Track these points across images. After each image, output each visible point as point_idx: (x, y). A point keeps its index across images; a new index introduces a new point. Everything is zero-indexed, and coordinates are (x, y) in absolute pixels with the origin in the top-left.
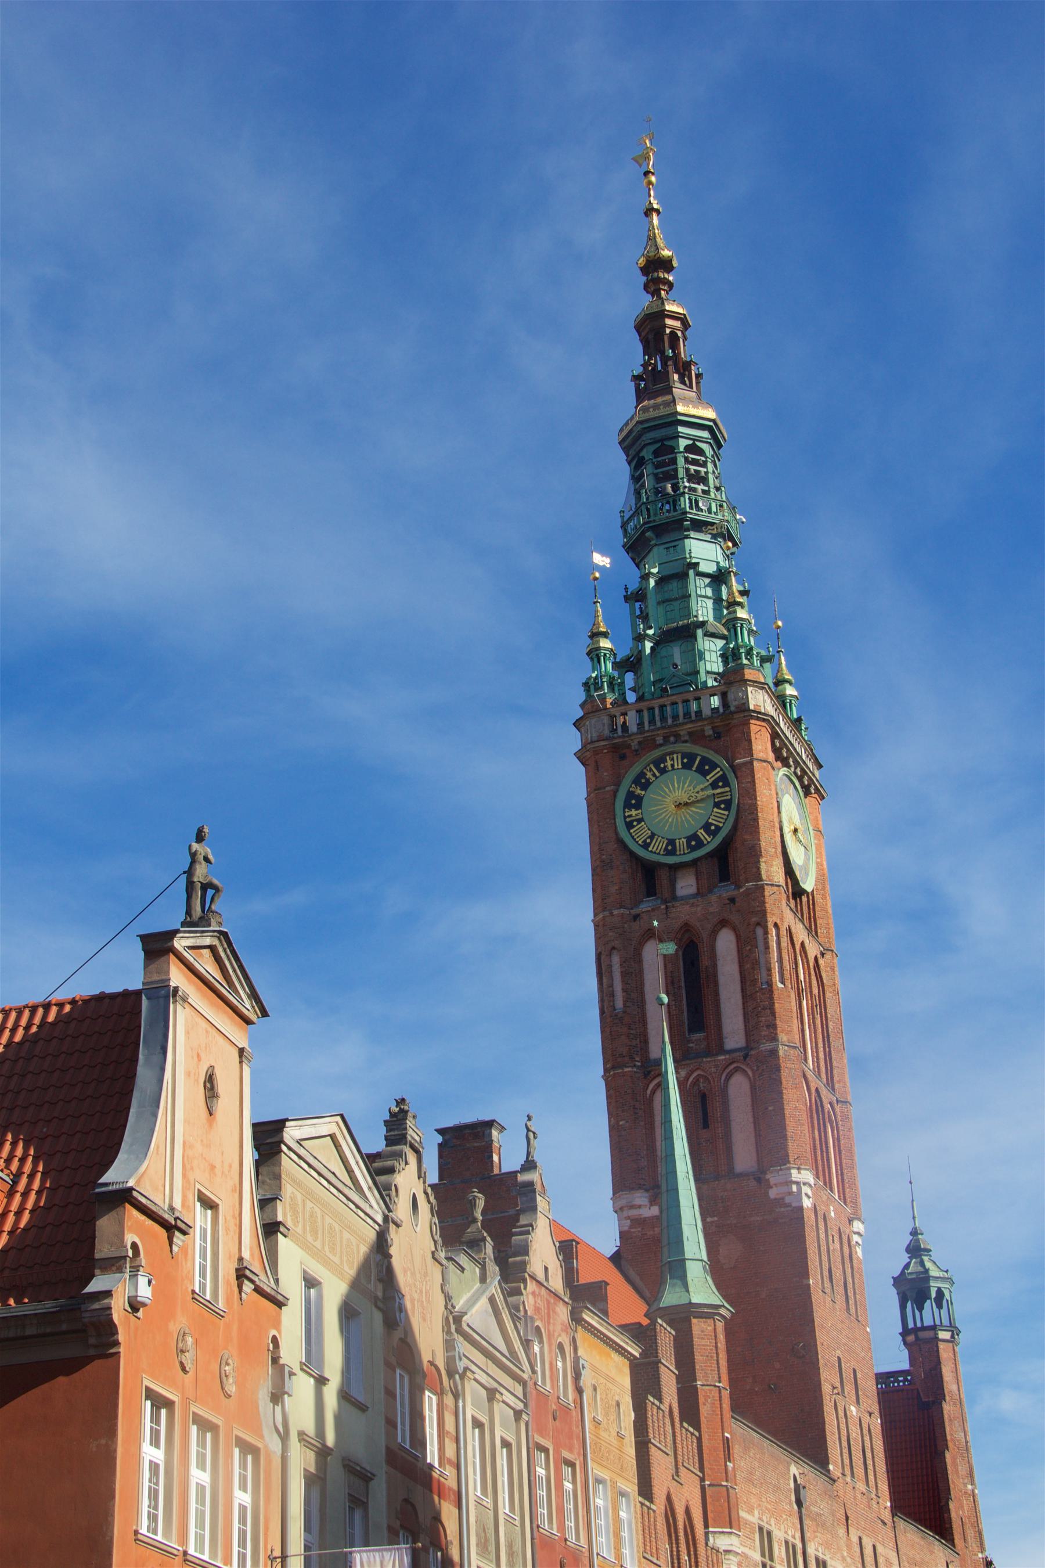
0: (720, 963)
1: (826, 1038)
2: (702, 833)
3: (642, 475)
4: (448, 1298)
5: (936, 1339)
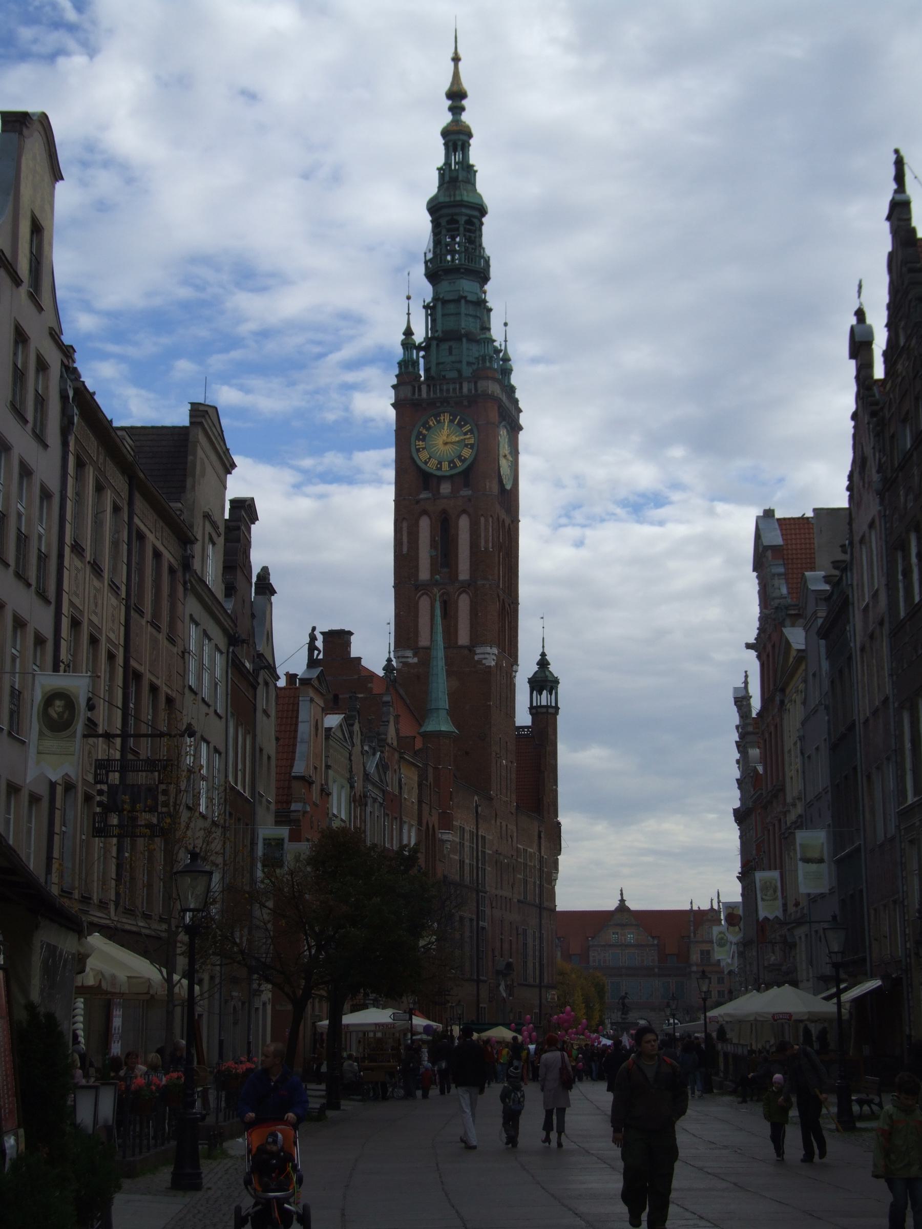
0: (460, 532)
3: (440, 233)
5: (547, 712)
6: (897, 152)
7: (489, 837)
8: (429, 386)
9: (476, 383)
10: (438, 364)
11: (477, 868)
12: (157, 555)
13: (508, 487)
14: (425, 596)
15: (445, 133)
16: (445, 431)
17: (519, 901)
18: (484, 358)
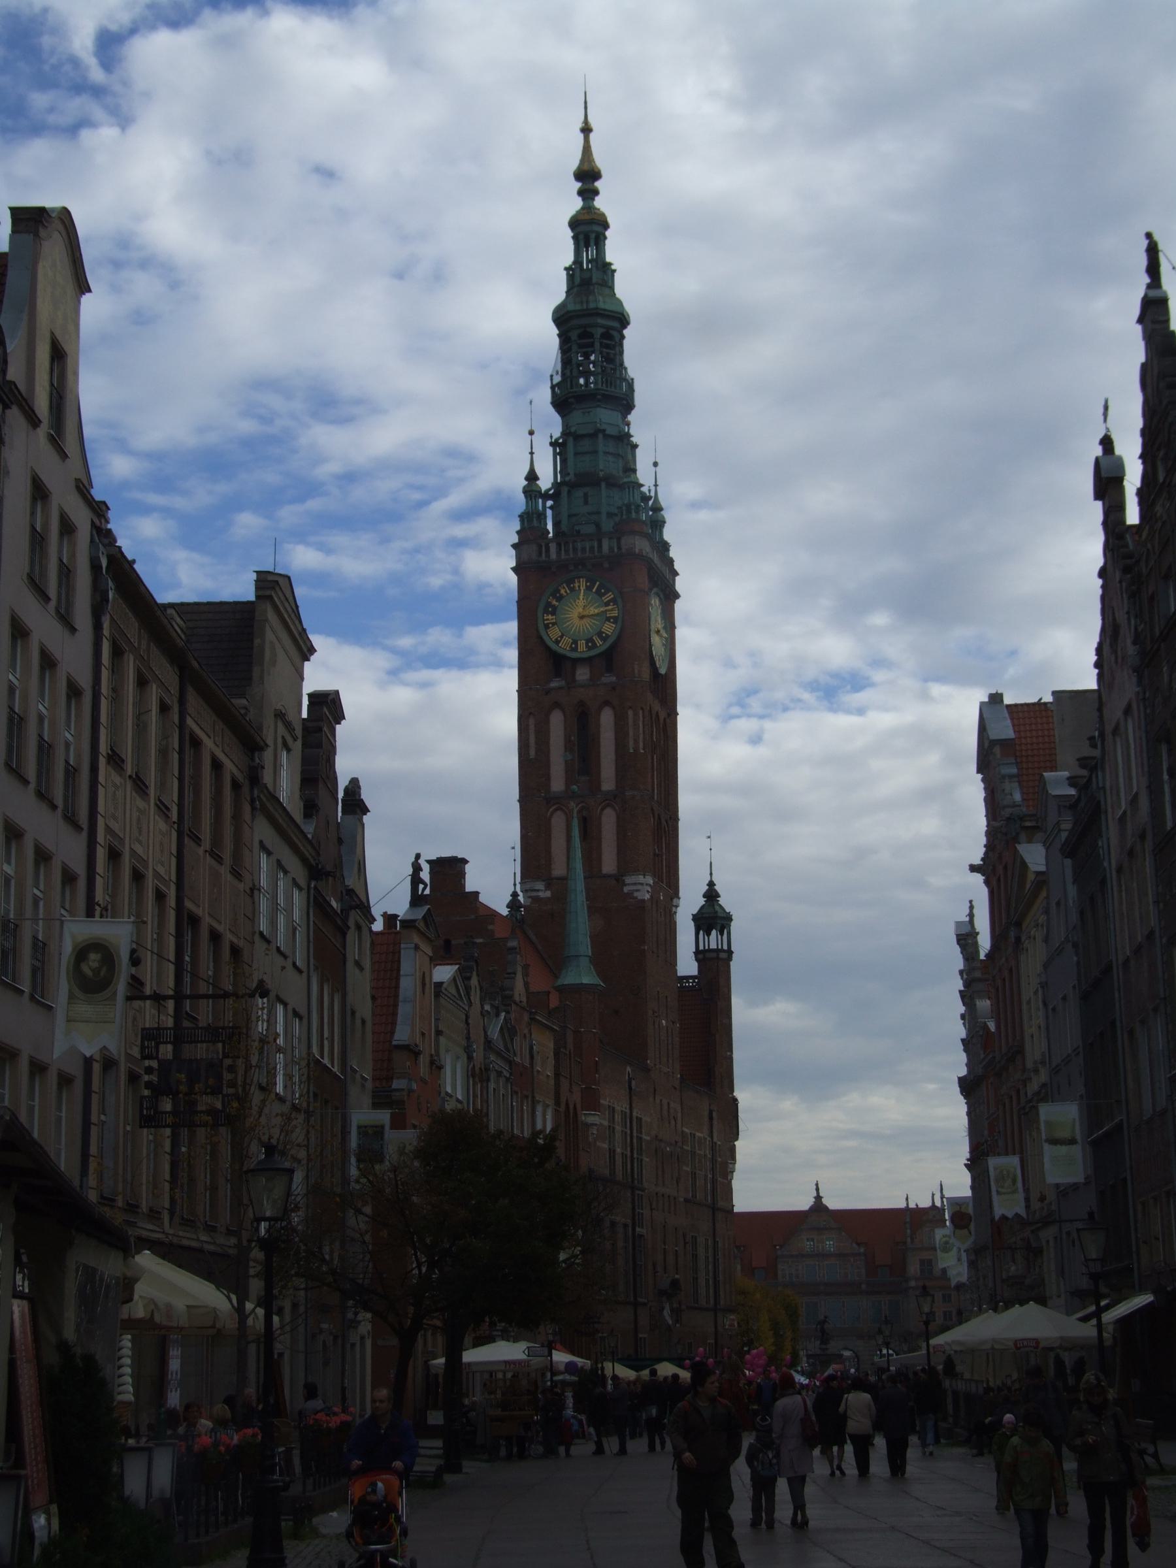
3: (570, 349)
4: (485, 1033)
5: (718, 958)
6: (1149, 236)
7: (646, 1119)
8: (559, 545)
9: (619, 539)
10: (570, 516)
12: (217, 765)
13: (663, 671)
14: (559, 813)
15: (574, 224)
16: (581, 600)
17: (686, 1200)
18: (628, 506)
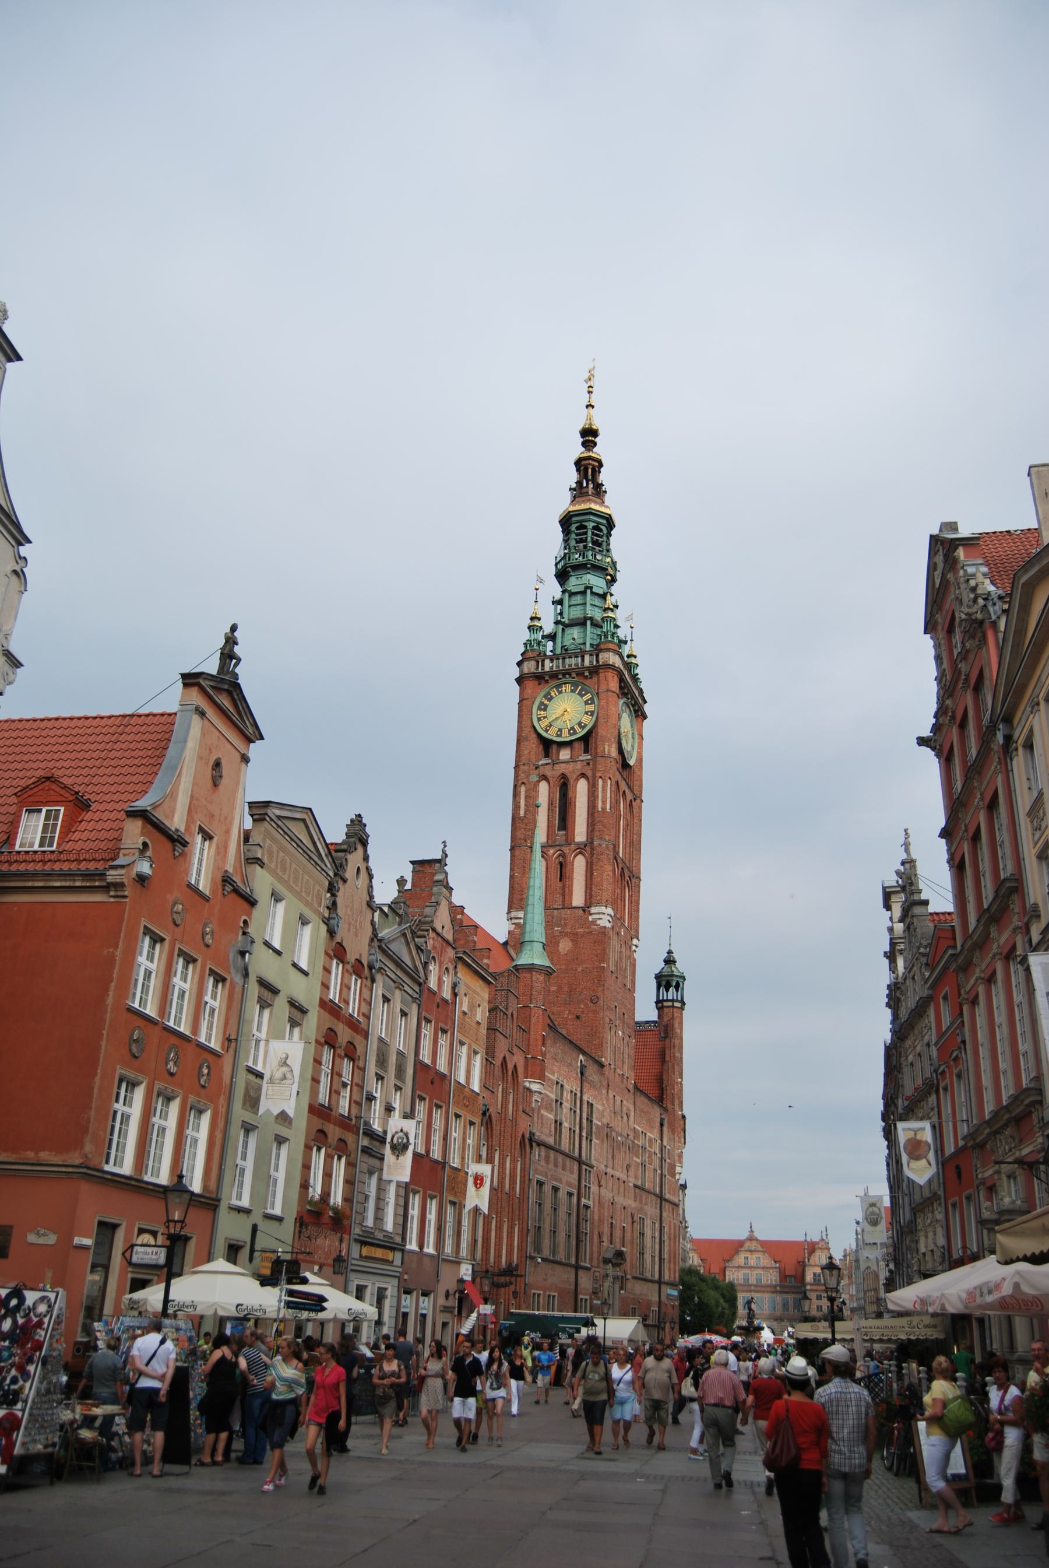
1: (632, 843)
2: (576, 727)
4: (374, 929)
5: (673, 1006)
7: (598, 1106)
9: (597, 656)
11: (581, 1136)
13: (632, 762)
15: (578, 463)
